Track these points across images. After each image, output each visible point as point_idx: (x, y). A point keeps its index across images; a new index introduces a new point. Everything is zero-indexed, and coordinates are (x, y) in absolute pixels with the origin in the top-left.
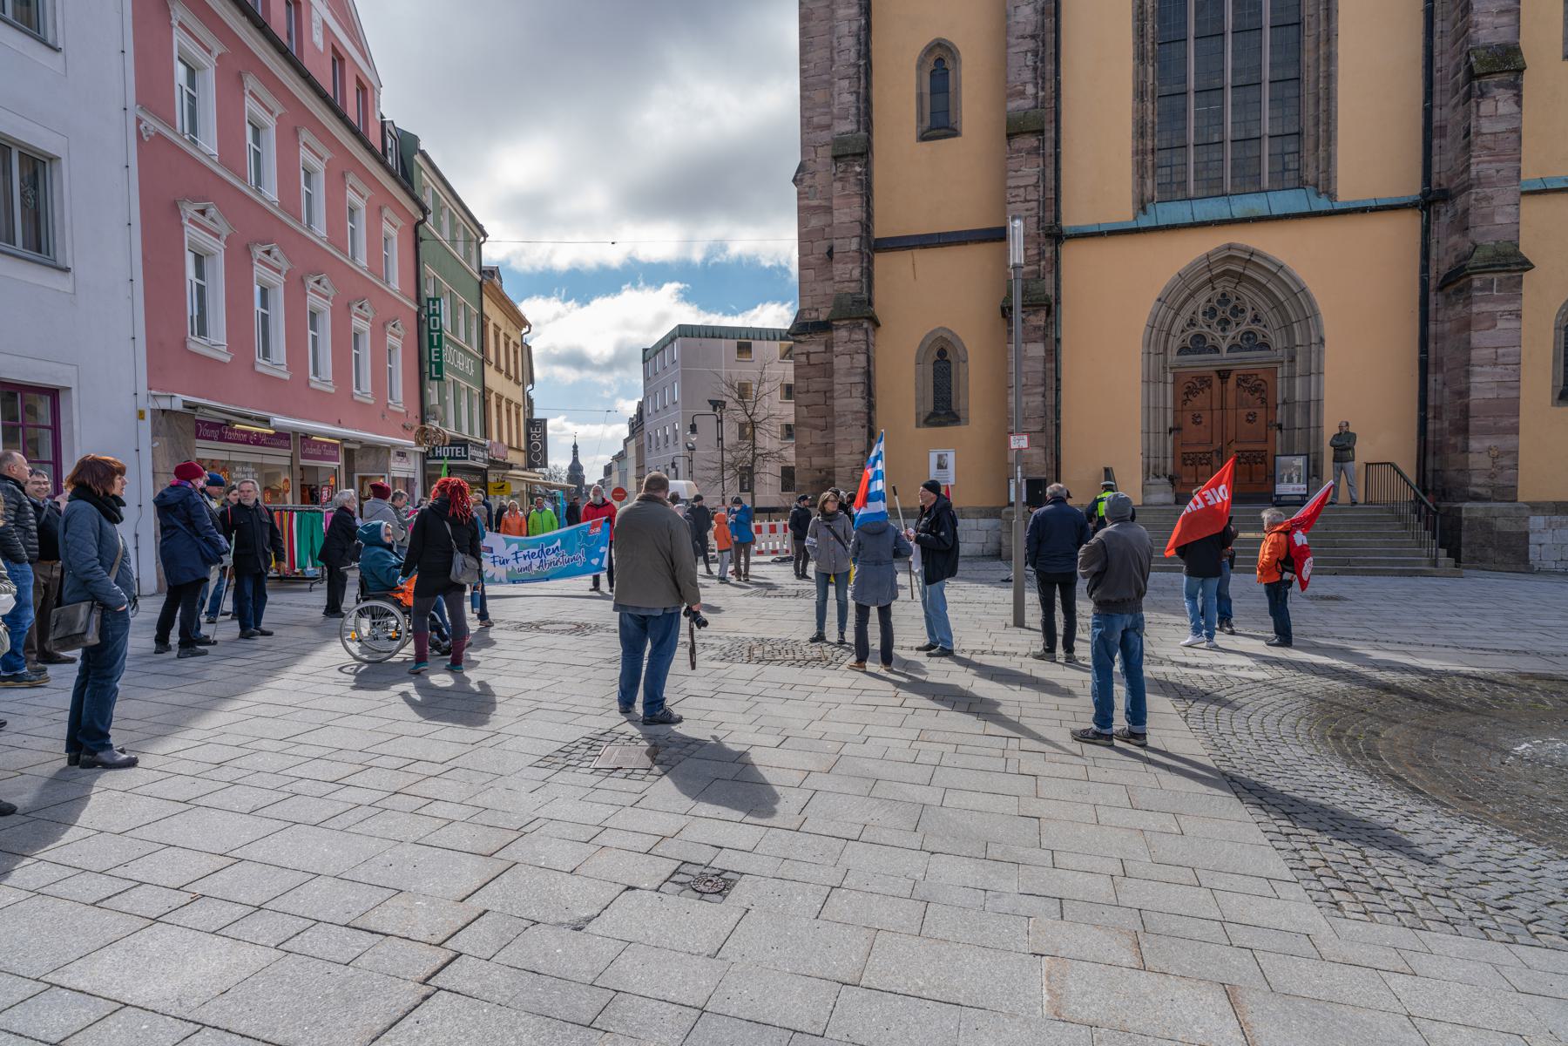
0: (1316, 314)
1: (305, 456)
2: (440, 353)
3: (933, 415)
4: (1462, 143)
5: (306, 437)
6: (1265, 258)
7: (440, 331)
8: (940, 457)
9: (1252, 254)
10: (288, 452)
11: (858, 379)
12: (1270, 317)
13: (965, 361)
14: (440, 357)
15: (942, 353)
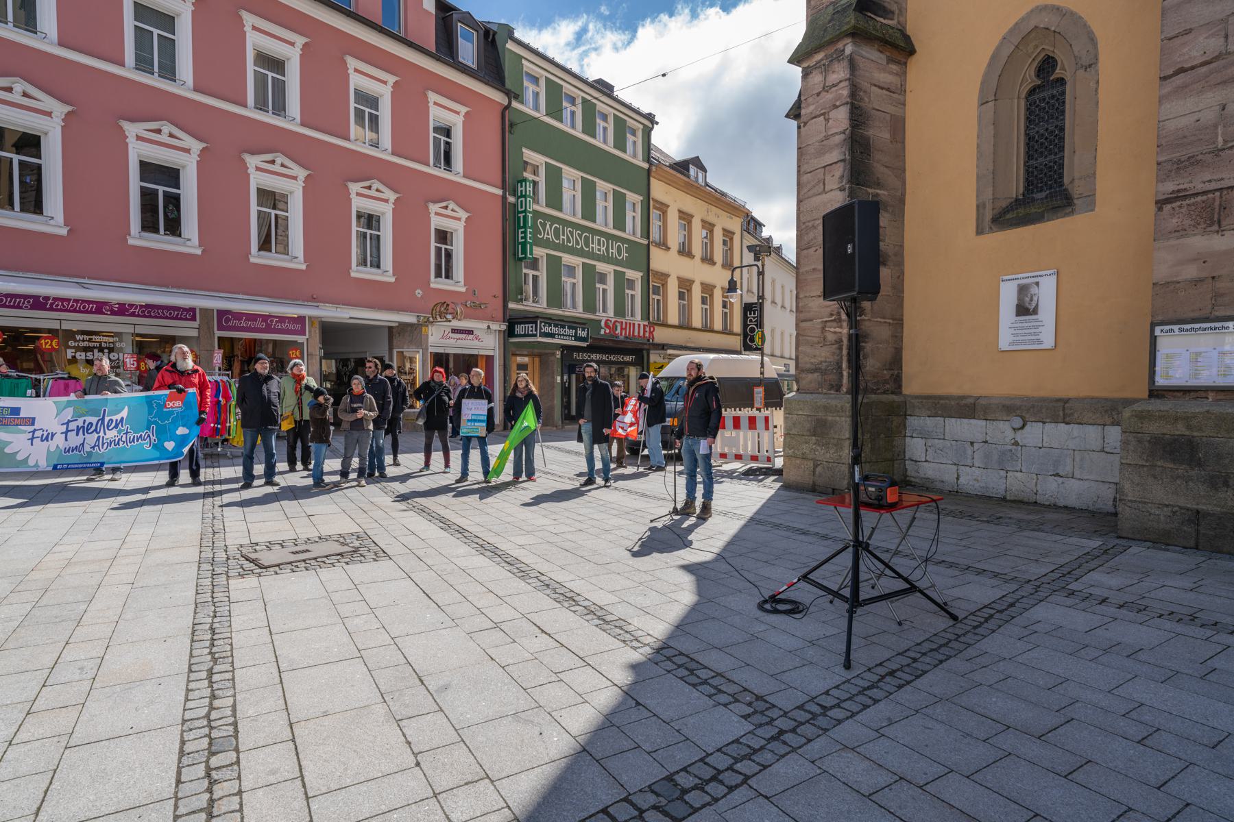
1: (220, 328)
2: (525, 233)
3: (1017, 203)
5: (222, 313)
7: (525, 211)
8: (1023, 290)
10: (196, 324)
11: (835, 156)
13: (1091, 65)
14: (525, 237)
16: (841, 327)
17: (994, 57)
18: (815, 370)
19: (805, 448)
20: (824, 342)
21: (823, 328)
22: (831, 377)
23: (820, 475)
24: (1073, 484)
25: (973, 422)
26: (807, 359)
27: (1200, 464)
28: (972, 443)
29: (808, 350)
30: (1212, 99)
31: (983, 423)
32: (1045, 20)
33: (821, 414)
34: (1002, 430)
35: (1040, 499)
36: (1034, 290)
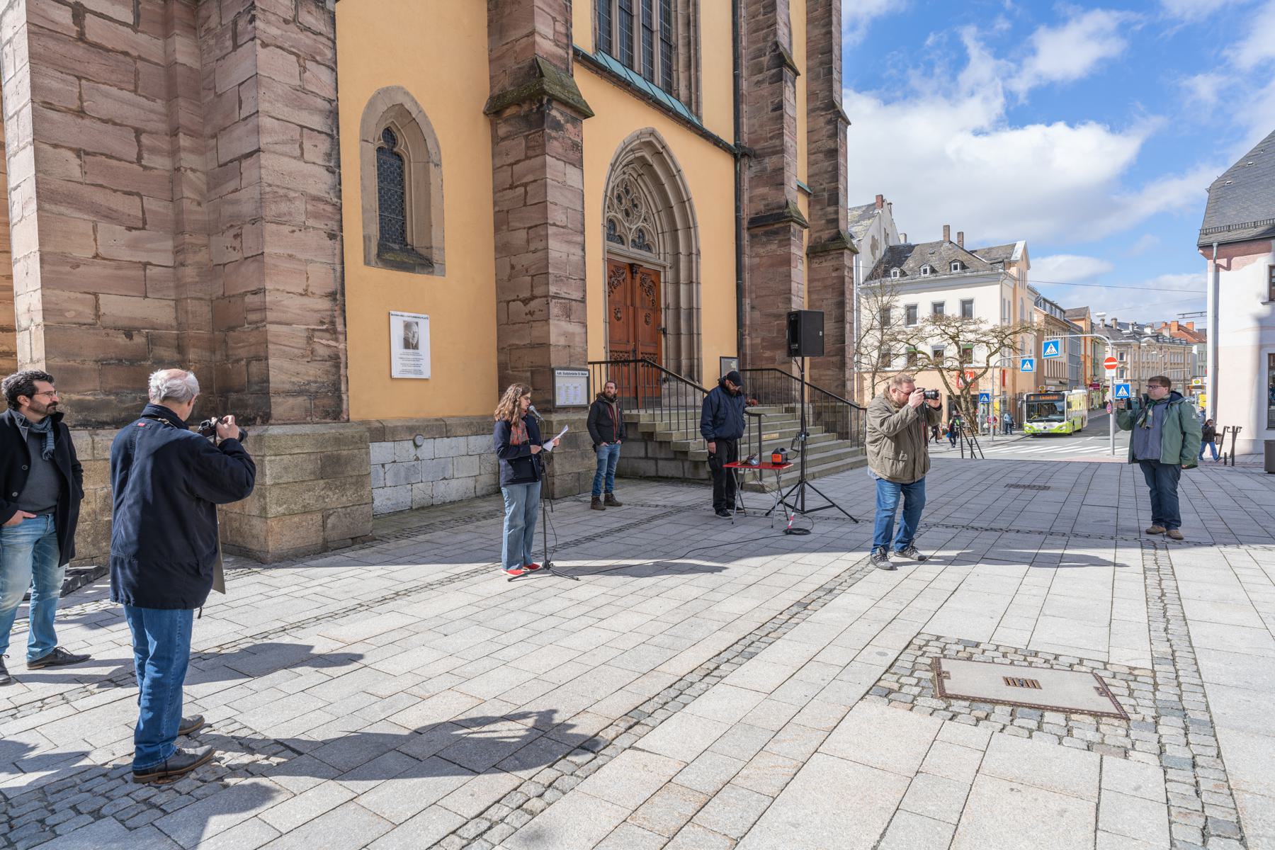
0: (695, 227)
4: (767, 113)
6: (671, 157)
8: (407, 326)
9: (663, 147)
12: (661, 222)
15: (389, 134)
16: (336, 340)
17: (371, 104)
18: (300, 393)
19: (309, 499)
20: (312, 356)
21: (310, 339)
22: (326, 401)
23: (334, 527)
24: (454, 483)
25: (384, 444)
26: (284, 377)
27: (578, 447)
28: (383, 465)
29: (286, 364)
30: (565, 247)
31: (391, 444)
32: (408, 106)
33: (330, 450)
34: (405, 449)
35: (435, 501)
36: (415, 328)
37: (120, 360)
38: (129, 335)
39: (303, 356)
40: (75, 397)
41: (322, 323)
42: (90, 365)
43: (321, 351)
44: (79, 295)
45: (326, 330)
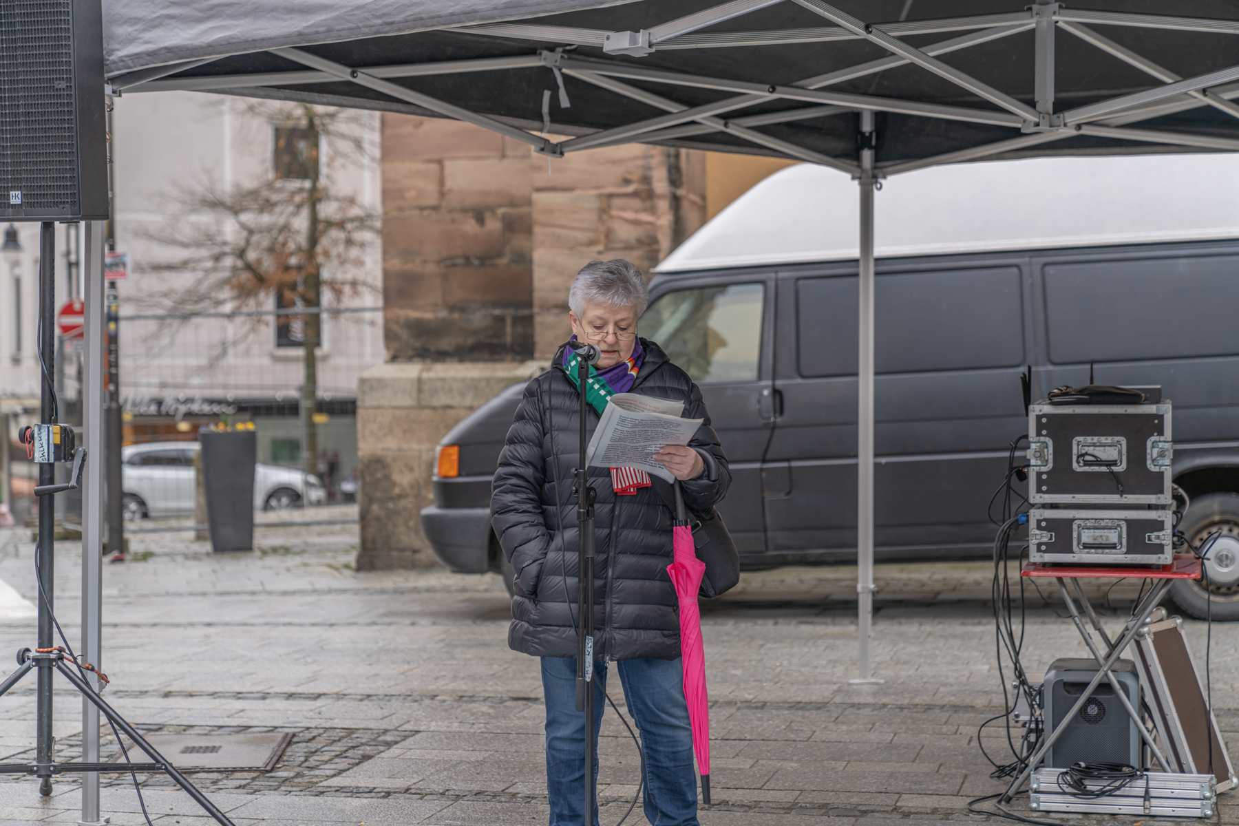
16: (652, 210)
21: (604, 211)
37: (467, 259)
38: (480, 220)
39: (592, 243)
40: (414, 314)
41: (627, 182)
42: (431, 268)
43: (624, 232)
44: (422, 166)
45: (635, 194)
